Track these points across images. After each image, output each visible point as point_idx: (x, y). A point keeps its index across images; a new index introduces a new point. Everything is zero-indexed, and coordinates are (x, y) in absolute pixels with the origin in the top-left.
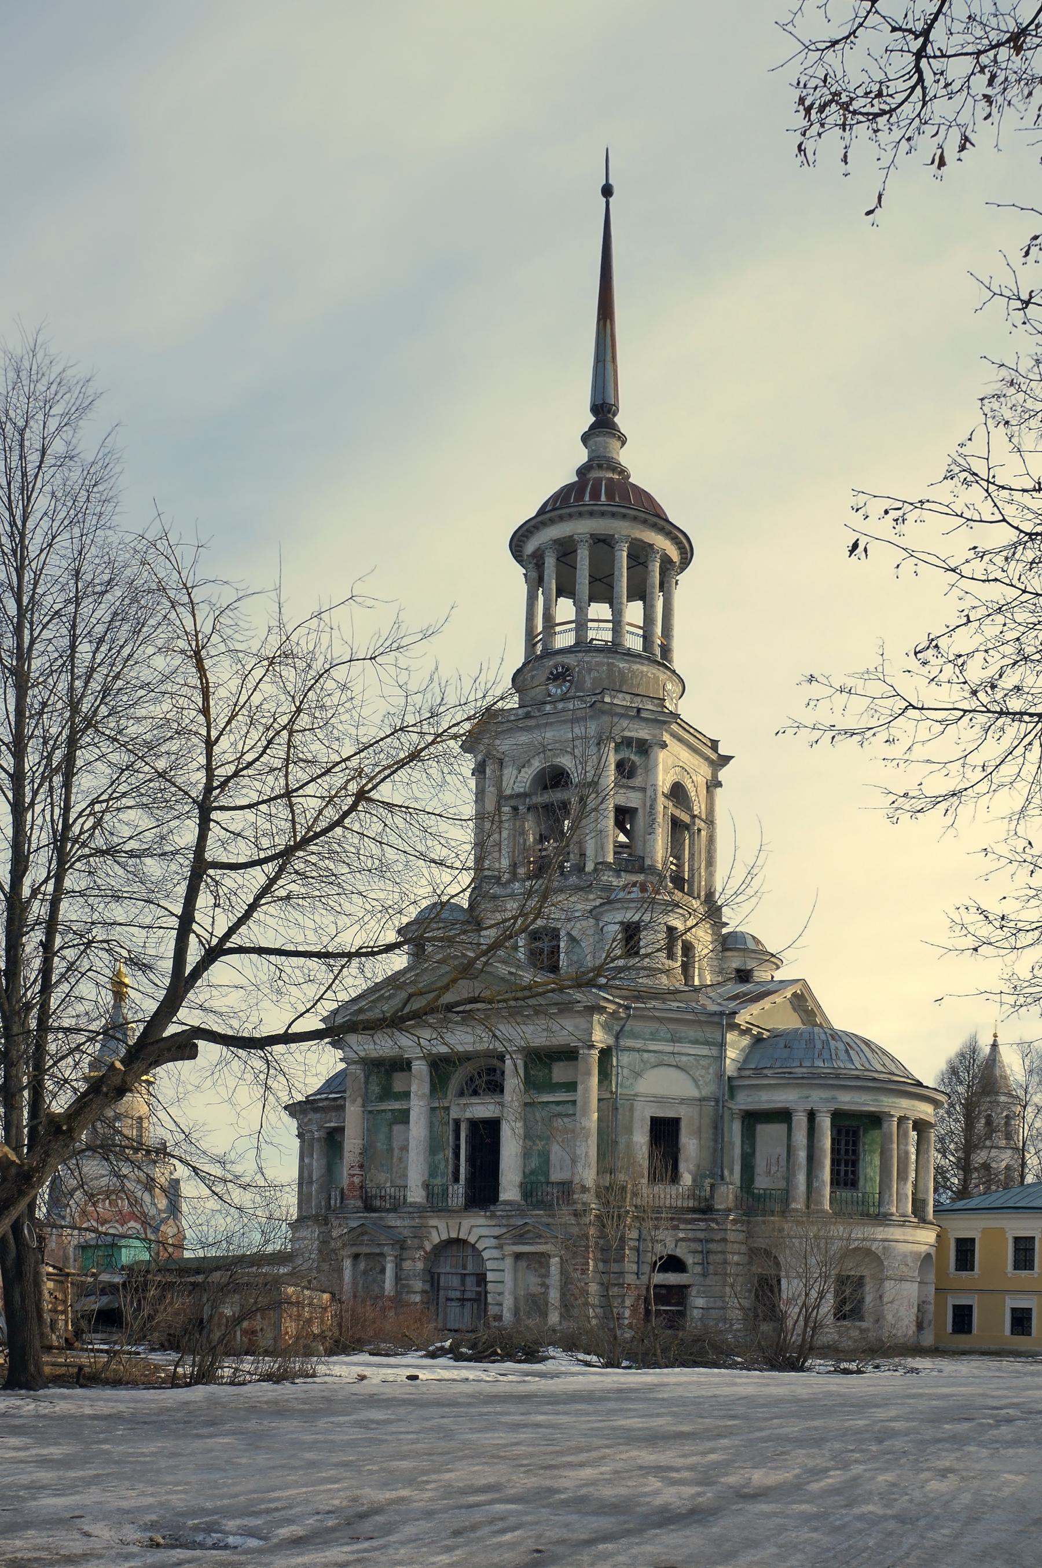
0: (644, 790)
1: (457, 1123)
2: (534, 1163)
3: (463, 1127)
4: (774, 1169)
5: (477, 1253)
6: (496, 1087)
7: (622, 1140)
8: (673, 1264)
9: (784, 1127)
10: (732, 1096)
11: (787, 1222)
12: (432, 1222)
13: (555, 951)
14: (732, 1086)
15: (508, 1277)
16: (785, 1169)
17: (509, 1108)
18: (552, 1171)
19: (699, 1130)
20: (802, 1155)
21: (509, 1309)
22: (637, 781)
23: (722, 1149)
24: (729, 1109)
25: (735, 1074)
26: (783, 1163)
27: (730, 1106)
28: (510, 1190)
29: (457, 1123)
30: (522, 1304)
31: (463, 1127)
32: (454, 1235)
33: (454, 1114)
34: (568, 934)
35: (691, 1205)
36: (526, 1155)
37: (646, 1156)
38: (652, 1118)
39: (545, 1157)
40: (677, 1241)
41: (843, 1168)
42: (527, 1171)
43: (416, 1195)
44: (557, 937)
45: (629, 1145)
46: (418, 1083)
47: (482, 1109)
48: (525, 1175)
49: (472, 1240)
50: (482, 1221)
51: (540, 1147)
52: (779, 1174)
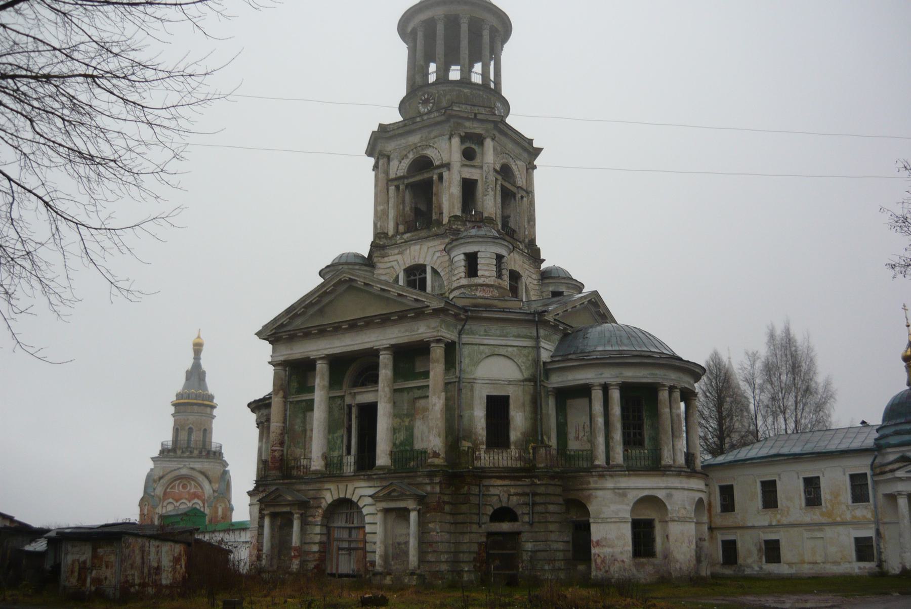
2: (402, 436)
3: (354, 410)
4: (581, 434)
5: (359, 510)
6: (374, 380)
7: (466, 414)
8: (504, 514)
9: (585, 401)
10: (547, 378)
11: (592, 476)
12: (327, 486)
13: (423, 281)
14: (547, 370)
15: (379, 529)
17: (381, 396)
18: (415, 442)
19: (524, 405)
20: (600, 420)
21: (381, 556)
22: (477, 162)
23: (541, 419)
25: (549, 360)
26: (587, 429)
28: (382, 459)
29: (350, 407)
30: (390, 551)
31: (354, 410)
32: (342, 496)
33: (348, 400)
35: (519, 466)
36: (395, 430)
37: (484, 426)
38: (488, 397)
39: (410, 430)
40: (509, 495)
41: (632, 431)
42: (397, 442)
43: (317, 464)
44: (425, 271)
45: (471, 418)
46: (320, 380)
47: (365, 397)
48: (394, 444)
49: (355, 499)
50: (363, 484)
51: (407, 424)
52: (585, 438)
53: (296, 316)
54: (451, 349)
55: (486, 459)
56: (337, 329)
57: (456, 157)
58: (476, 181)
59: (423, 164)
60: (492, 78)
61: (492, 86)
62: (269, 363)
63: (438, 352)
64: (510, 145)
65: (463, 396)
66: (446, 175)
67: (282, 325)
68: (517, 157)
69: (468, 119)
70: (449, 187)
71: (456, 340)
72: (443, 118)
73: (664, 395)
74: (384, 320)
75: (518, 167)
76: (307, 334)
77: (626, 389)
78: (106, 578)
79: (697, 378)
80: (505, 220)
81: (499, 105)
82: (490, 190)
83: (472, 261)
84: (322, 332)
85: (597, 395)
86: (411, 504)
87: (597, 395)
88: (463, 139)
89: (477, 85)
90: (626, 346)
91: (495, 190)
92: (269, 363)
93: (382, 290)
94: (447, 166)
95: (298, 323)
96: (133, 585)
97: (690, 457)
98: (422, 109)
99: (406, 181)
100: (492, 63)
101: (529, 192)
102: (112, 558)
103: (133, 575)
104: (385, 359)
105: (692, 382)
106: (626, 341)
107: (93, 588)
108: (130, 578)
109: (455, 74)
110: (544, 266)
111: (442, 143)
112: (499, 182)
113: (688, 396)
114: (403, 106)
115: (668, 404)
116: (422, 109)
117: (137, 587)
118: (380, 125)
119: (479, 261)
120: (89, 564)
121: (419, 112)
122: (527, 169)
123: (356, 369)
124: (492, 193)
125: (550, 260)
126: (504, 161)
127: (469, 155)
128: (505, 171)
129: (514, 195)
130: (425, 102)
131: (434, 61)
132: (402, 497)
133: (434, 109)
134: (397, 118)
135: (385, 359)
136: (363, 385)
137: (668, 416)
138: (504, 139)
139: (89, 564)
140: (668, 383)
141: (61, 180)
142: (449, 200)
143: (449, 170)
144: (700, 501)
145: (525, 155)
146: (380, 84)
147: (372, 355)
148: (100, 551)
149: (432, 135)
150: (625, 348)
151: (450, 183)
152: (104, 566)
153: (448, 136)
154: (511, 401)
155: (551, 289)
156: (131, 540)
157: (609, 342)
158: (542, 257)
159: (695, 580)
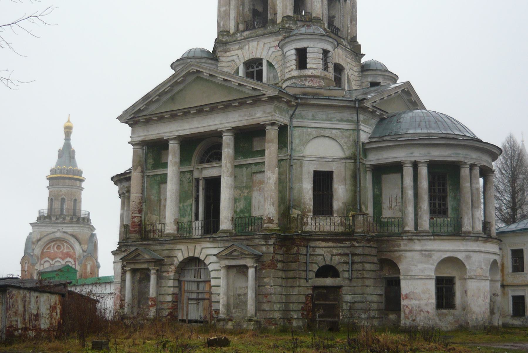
1: (197, 180)
2: (241, 205)
4: (394, 204)
5: (206, 266)
6: (218, 157)
7: (296, 186)
8: (327, 271)
9: (398, 176)
10: (365, 156)
11: (403, 240)
12: (179, 246)
15: (222, 282)
16: (400, 204)
17: (224, 170)
18: (253, 210)
19: (345, 179)
20: (410, 193)
21: (223, 305)
23: (360, 191)
24: (363, 164)
25: (367, 141)
26: (399, 200)
27: (364, 162)
28: (225, 223)
29: (197, 180)
30: (232, 301)
32: (191, 255)
33: (196, 174)
34: (268, 61)
35: (340, 230)
36: (236, 200)
37: (312, 197)
38: (314, 171)
39: (249, 200)
40: (332, 255)
41: (437, 202)
42: (238, 210)
43: (170, 228)
44: (261, 64)
45: (301, 191)
46: (173, 157)
47: (210, 172)
48: (235, 212)
49: (202, 258)
50: (209, 245)
51: (246, 194)
52: (397, 208)
53: (151, 102)
55: (313, 224)
56: (186, 113)
63: (272, 133)
65: (294, 171)
67: (140, 111)
71: (288, 124)
73: (465, 172)
74: (226, 106)
76: (161, 118)
77: (432, 165)
79: (494, 157)
83: (302, 54)
84: (174, 116)
85: (408, 171)
86: (249, 262)
87: (408, 171)
90: (433, 129)
93: (225, 80)
95: (153, 108)
96: (17, 330)
97: (486, 225)
103: (16, 321)
104: (228, 140)
105: (490, 160)
106: (433, 125)
108: (14, 323)
110: (363, 60)
113: (486, 172)
115: (468, 179)
117: (20, 331)
119: (308, 55)
123: (203, 148)
125: (369, 55)
135: (228, 140)
136: (208, 161)
137: (469, 189)
140: (469, 162)
144: (495, 262)
147: (217, 135)
150: (433, 131)
154: (335, 176)
155: (370, 80)
156: (14, 292)
157: (419, 125)
158: (362, 52)
159: (489, 329)
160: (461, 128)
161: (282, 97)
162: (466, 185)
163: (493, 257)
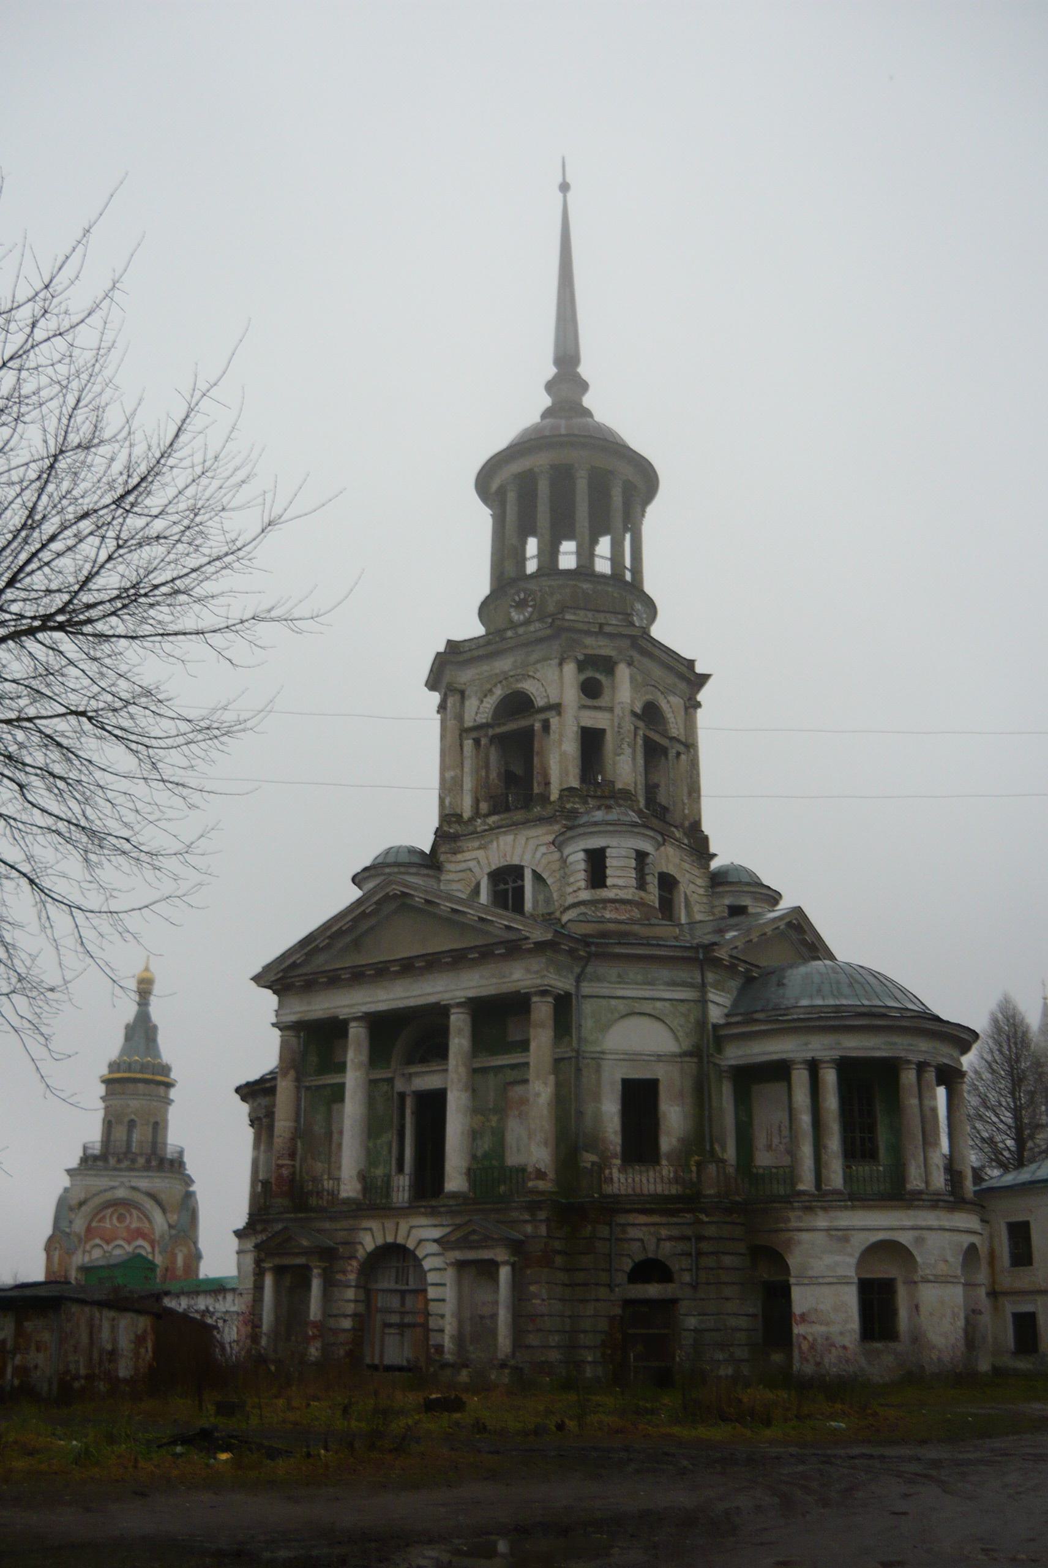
0: (611, 710)
2: (485, 1144)
3: (409, 1103)
4: (776, 1141)
5: (418, 1262)
8: (650, 1270)
9: (781, 1086)
10: (719, 1050)
11: (793, 1209)
12: (366, 1224)
13: (520, 892)
15: (449, 1293)
16: (787, 1140)
17: (453, 1079)
20: (805, 1119)
22: (603, 701)
24: (715, 1064)
25: (722, 1021)
26: (785, 1132)
27: (717, 1061)
28: (455, 1181)
29: (402, 1096)
31: (409, 1103)
32: (390, 1240)
33: (400, 1086)
34: (534, 871)
35: (674, 1192)
36: (474, 1135)
39: (499, 1136)
40: (659, 1240)
42: (479, 1153)
43: (349, 1188)
44: (521, 877)
46: (355, 1054)
47: (427, 1081)
48: (474, 1157)
49: (411, 1245)
50: (423, 1221)
51: (494, 1124)
52: (782, 1147)
53: (317, 950)
54: (563, 1005)
55: (621, 1181)
56: (381, 973)
57: (571, 696)
58: (604, 731)
59: (517, 704)
60: (628, 564)
61: (628, 576)
62: (273, 1025)
63: (543, 1010)
64: (657, 672)
66: (554, 721)
67: (294, 966)
68: (667, 691)
69: (588, 633)
70: (560, 742)
71: (573, 990)
72: (549, 632)
73: (909, 1077)
74: (458, 960)
75: (671, 706)
76: (334, 981)
77: (846, 1067)
78: (36, 1367)
79: (965, 1048)
80: (651, 799)
81: (638, 606)
82: (625, 746)
83: (597, 861)
84: (358, 977)
86: (500, 1254)
87: (800, 1078)
88: (581, 666)
89: (603, 576)
90: (846, 998)
91: (633, 746)
92: (273, 1025)
93: (454, 911)
94: (557, 708)
95: (320, 962)
96: (77, 1377)
98: (516, 616)
99: (491, 732)
100: (628, 536)
101: (690, 746)
102: (46, 1336)
103: (77, 1362)
104: (458, 1021)
105: (955, 1054)
106: (846, 990)
107: (16, 1382)
108: (72, 1367)
109: (568, 557)
110: (714, 864)
111: (549, 672)
112: (641, 733)
113: (950, 1076)
114: (485, 610)
115: (915, 1089)
116: (516, 616)
117: (83, 1381)
118: (449, 642)
119: (609, 862)
120: (10, 1345)
121: (511, 621)
122: (686, 708)
124: (628, 751)
126: (649, 697)
127: (591, 690)
128: (651, 714)
129: (665, 751)
130: (521, 605)
131: (533, 533)
132: (486, 1242)
133: (535, 617)
134: (477, 630)
135: (458, 1021)
136: (423, 1061)
137: (916, 1110)
138: (647, 662)
139: (10, 1345)
140: (915, 1058)
141: (63, 868)
142: (560, 761)
143: (559, 714)
144: (972, 1248)
145: (682, 686)
146: (448, 581)
147: (438, 1013)
148: (29, 1325)
149: (534, 657)
150: (845, 1002)
151: (561, 735)
152: (33, 1348)
153: (556, 661)
155: (727, 902)
156: (75, 1308)
157: (819, 991)
158: (712, 850)
159: (962, 1378)
160: (899, 995)
161: (560, 943)
162: (912, 1102)
163: (967, 1240)
